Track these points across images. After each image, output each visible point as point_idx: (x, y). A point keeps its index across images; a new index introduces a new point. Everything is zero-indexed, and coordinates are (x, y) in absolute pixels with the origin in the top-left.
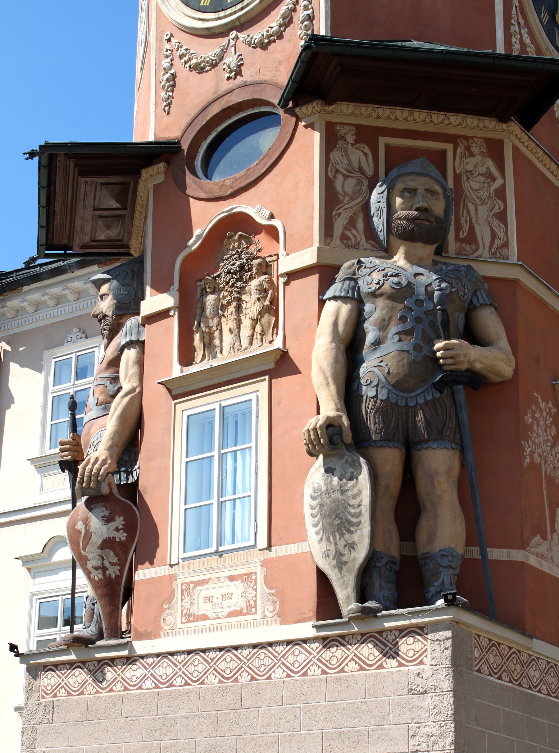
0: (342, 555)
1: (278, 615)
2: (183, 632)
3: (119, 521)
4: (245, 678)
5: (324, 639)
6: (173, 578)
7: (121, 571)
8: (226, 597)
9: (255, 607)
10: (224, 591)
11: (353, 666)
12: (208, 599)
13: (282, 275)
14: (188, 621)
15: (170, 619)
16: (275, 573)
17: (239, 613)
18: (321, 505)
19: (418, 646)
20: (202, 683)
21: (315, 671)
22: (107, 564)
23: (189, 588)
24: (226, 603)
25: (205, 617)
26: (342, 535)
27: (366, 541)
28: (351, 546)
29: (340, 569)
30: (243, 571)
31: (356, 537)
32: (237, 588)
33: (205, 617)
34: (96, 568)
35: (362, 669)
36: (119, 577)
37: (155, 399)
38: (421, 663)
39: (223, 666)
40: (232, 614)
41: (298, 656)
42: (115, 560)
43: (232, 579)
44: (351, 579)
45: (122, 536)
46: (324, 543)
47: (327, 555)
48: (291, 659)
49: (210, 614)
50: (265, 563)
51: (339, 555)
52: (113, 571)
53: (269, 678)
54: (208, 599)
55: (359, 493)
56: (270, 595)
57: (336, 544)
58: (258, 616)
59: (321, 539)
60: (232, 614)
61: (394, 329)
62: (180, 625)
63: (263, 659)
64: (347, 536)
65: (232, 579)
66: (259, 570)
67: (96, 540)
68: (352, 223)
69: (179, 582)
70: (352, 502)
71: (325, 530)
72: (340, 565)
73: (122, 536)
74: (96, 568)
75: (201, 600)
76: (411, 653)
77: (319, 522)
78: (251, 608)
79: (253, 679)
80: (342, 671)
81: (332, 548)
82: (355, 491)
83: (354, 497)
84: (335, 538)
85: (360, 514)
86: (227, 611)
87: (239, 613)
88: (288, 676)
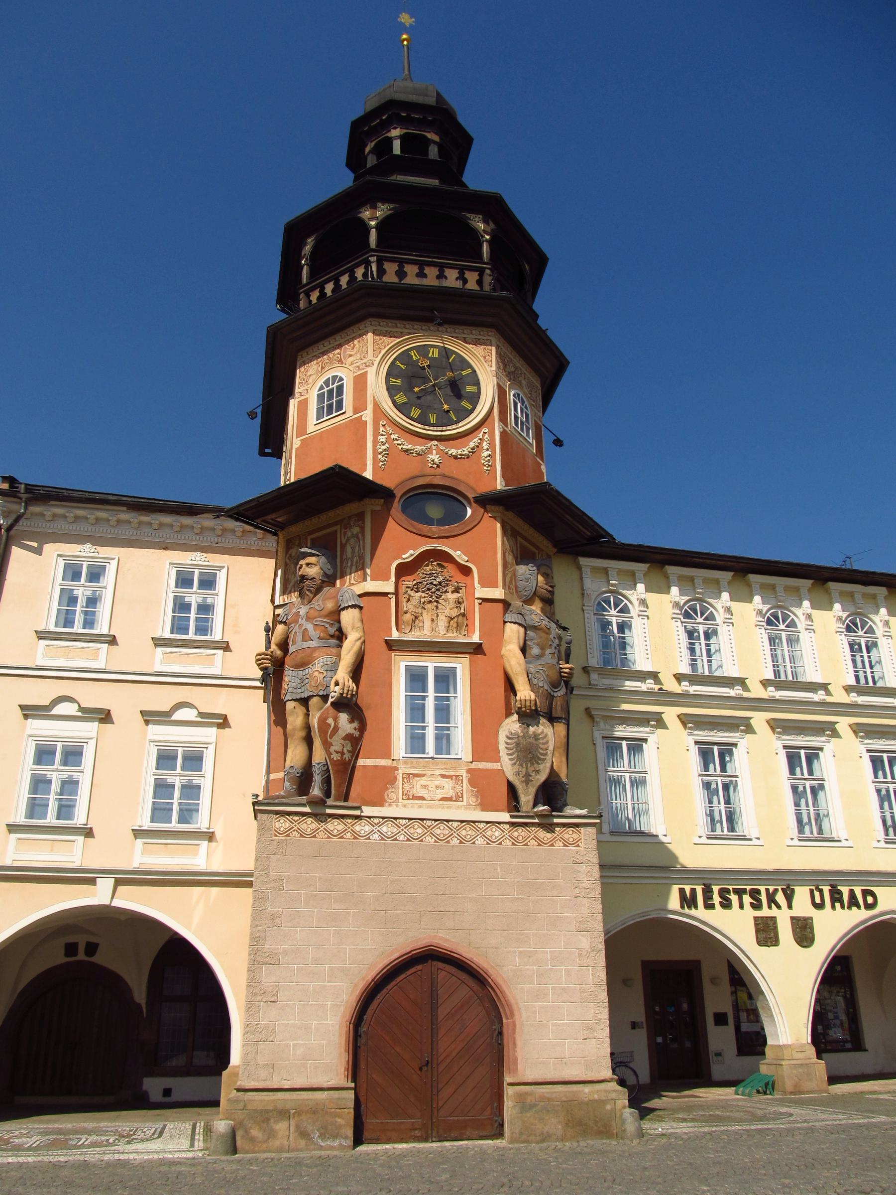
0: (530, 776)
1: (480, 804)
2: (405, 806)
3: (356, 724)
4: (455, 841)
6: (396, 768)
7: (352, 757)
9: (462, 797)
10: (437, 783)
12: (425, 787)
13: (478, 599)
14: (409, 799)
15: (393, 795)
16: (475, 777)
17: (450, 799)
18: (518, 744)
19: (575, 836)
20: (422, 841)
22: (345, 751)
23: (408, 777)
24: (439, 791)
25: (422, 798)
26: (532, 764)
27: (548, 771)
28: (538, 772)
29: (527, 784)
30: (453, 773)
31: (541, 767)
32: (448, 784)
33: (422, 798)
34: (337, 752)
35: (539, 845)
36: (350, 761)
37: (376, 650)
38: (578, 846)
39: (438, 831)
40: (443, 799)
41: (495, 833)
42: (350, 748)
43: (443, 776)
44: (532, 790)
45: (357, 734)
46: (516, 767)
47: (517, 774)
48: (489, 833)
49: (426, 796)
50: (469, 771)
51: (527, 775)
52: (347, 756)
53: (474, 843)
54: (425, 787)
55: (547, 742)
56: (473, 791)
57: (527, 768)
58: (465, 803)
59: (514, 764)
60: (443, 799)
61: (548, 651)
62: (401, 800)
63: (467, 832)
64: (536, 765)
65: (443, 776)
66: (464, 775)
67: (341, 733)
68: (511, 580)
69: (400, 772)
70: (542, 746)
71: (518, 758)
72: (527, 781)
73: (357, 734)
74: (337, 752)
75: (419, 787)
76: (571, 840)
77: (513, 753)
78: (459, 797)
79: (461, 842)
80: (526, 845)
81: (524, 770)
82: (545, 740)
83: (544, 744)
84: (527, 765)
85: (546, 754)
86: (440, 796)
87: (450, 799)
88: (488, 844)
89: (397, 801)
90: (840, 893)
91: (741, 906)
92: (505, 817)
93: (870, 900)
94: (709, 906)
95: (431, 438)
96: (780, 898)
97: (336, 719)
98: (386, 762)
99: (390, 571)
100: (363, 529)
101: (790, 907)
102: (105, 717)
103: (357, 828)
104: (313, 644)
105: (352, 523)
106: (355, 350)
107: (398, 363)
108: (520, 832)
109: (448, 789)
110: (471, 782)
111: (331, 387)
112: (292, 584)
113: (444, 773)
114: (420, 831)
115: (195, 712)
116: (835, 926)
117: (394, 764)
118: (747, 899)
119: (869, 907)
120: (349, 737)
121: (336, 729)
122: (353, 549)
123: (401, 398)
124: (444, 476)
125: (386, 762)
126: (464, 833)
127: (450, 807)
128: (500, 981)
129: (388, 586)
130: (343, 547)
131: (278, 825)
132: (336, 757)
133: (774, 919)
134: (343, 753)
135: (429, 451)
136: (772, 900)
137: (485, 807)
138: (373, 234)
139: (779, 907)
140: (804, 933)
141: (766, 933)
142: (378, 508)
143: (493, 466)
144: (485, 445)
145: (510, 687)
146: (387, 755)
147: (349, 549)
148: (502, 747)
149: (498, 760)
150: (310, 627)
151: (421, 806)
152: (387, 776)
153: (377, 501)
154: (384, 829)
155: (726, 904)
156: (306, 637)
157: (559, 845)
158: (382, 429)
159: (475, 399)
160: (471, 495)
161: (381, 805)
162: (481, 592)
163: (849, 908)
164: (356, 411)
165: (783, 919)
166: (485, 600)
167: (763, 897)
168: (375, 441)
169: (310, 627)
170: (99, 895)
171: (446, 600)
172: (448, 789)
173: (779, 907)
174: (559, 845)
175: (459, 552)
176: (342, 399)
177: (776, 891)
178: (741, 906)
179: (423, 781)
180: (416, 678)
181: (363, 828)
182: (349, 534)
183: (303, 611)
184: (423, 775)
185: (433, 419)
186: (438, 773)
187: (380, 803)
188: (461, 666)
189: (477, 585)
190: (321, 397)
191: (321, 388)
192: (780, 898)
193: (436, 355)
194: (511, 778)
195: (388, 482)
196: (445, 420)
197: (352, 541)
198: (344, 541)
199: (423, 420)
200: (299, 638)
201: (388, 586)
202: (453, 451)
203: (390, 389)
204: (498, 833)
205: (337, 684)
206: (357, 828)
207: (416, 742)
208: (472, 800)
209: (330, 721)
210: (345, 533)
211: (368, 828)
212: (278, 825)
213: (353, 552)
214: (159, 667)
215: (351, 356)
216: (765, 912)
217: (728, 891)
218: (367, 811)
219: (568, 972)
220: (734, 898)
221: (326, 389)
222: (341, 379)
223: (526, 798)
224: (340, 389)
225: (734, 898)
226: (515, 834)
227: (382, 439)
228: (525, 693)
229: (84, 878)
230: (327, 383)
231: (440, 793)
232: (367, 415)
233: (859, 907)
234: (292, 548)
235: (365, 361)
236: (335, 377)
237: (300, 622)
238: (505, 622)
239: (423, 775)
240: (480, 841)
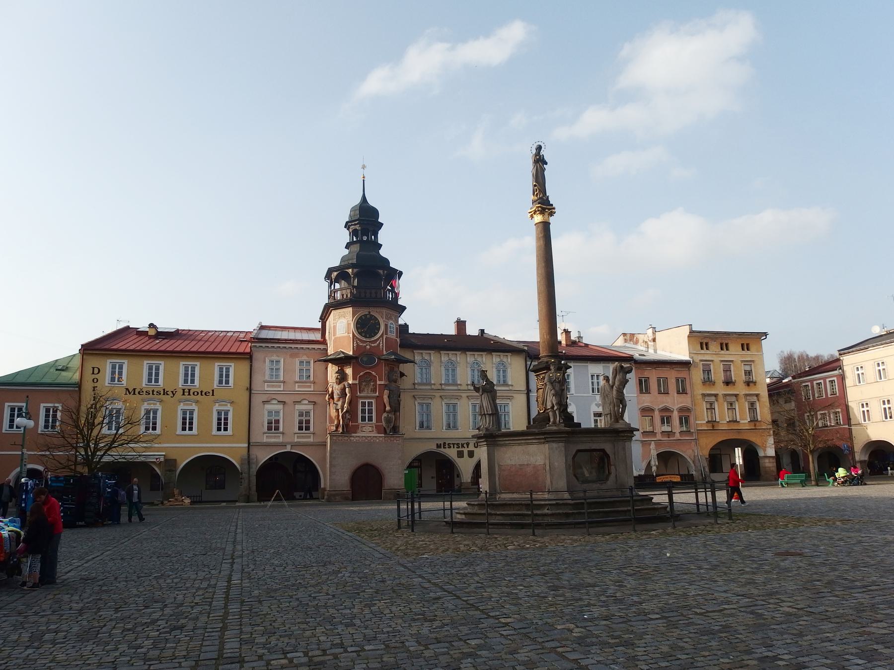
102: (284, 403)
109: (370, 429)
136: (463, 446)
141: (460, 455)
145: (385, 407)
152: (357, 427)
155: (450, 447)
159: (379, 329)
165: (466, 451)
170: (288, 449)
172: (370, 429)
180: (364, 404)
188: (373, 401)
196: (371, 337)
199: (365, 337)
207: (363, 419)
223: (388, 431)
228: (388, 408)
229: (283, 445)
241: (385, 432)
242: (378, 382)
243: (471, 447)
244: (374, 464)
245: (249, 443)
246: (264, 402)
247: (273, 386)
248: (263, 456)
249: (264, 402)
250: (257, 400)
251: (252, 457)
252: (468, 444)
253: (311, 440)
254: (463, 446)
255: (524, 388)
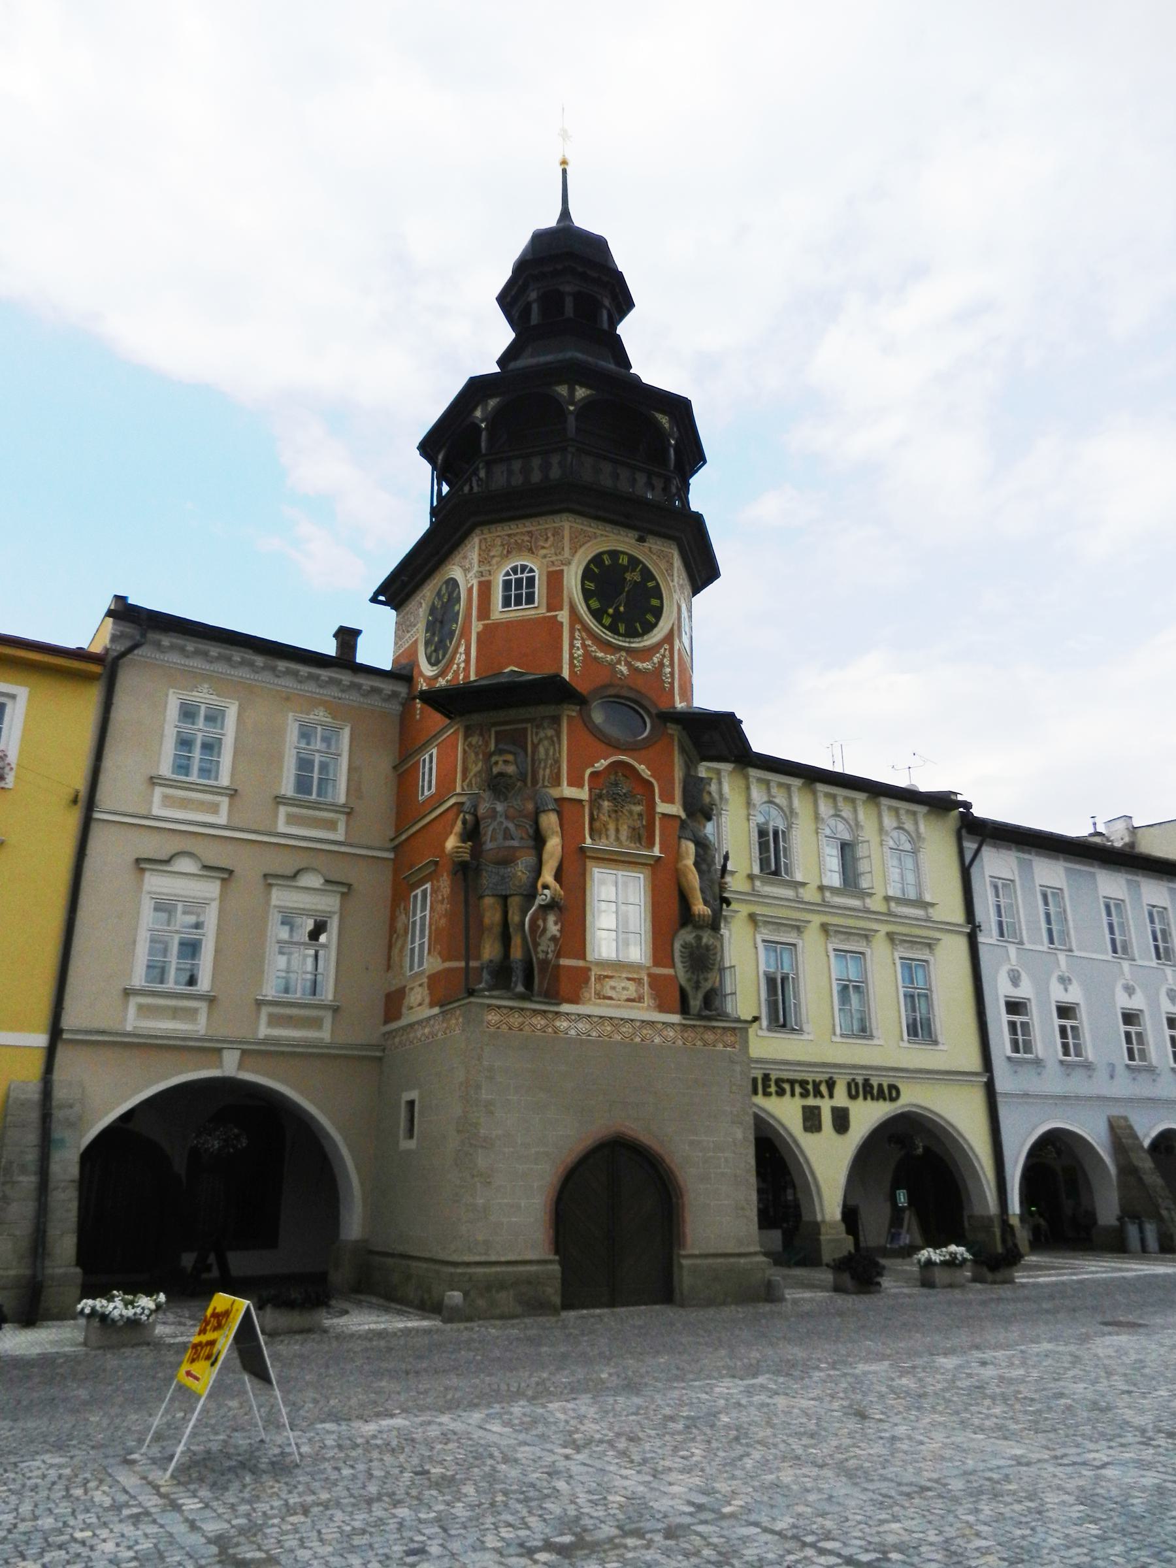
2: (595, 1004)
5: (684, 1025)
6: (589, 969)
8: (624, 988)
11: (699, 1043)
12: (613, 988)
15: (586, 995)
19: (733, 1039)
21: (680, 1042)
23: (600, 978)
25: (610, 998)
28: (706, 980)
32: (632, 986)
33: (610, 998)
40: (628, 1000)
45: (558, 934)
46: (689, 975)
47: (689, 980)
50: (649, 975)
54: (613, 988)
60: (628, 1000)
65: (629, 979)
67: (549, 935)
73: (558, 934)
78: (640, 999)
89: (590, 999)
90: (872, 1087)
91: (793, 1095)
92: (675, 1018)
93: (894, 1094)
94: (766, 1094)
95: (621, 648)
96: (824, 1089)
97: (545, 920)
98: (581, 963)
99: (583, 778)
100: (558, 734)
101: (831, 1096)
103: (558, 1024)
104: (515, 843)
105: (545, 724)
106: (549, 543)
107: (592, 566)
108: (689, 1034)
110: (651, 986)
111: (519, 576)
112: (472, 774)
113: (630, 976)
114: (609, 1028)
115: (322, 881)
116: (867, 1116)
117: (588, 965)
118: (798, 1090)
119: (892, 1099)
120: (554, 939)
121: (545, 930)
122: (547, 751)
123: (595, 604)
124: (631, 689)
125: (581, 963)
126: (645, 1032)
127: (632, 1008)
128: (673, 1166)
129: (583, 794)
130: (535, 747)
131: (490, 1017)
132: (541, 956)
133: (818, 1108)
134: (547, 953)
135: (619, 662)
137: (662, 1008)
138: (572, 422)
139: (822, 1096)
140: (841, 1121)
141: (812, 1121)
142: (574, 714)
143: (672, 684)
144: (666, 662)
146: (583, 956)
147: (541, 750)
148: (677, 954)
149: (673, 966)
150: (511, 826)
151: (609, 1006)
152: (582, 976)
153: (573, 707)
154: (580, 1025)
155: (781, 1093)
156: (507, 835)
157: (720, 1047)
158: (577, 633)
160: (654, 711)
161: (577, 1003)
162: (662, 808)
163: (878, 1099)
164: (549, 609)
165: (825, 1106)
166: (664, 815)
167: (810, 1087)
168: (572, 646)
169: (511, 826)
170: (229, 1066)
171: (631, 812)
173: (822, 1096)
174: (720, 1047)
175: (643, 767)
176: (534, 593)
177: (821, 1082)
178: (793, 1095)
179: (612, 983)
181: (563, 1024)
182: (542, 735)
183: (500, 807)
184: (611, 977)
185: (622, 629)
186: (624, 975)
187: (575, 1001)
189: (657, 800)
190: (507, 585)
191: (508, 574)
192: (824, 1089)
193: (625, 562)
194: (683, 982)
195: (583, 687)
196: (632, 634)
197: (546, 743)
198: (536, 741)
199: (613, 629)
200: (500, 836)
201: (583, 794)
202: (639, 665)
203: (587, 595)
204: (671, 1034)
205: (546, 887)
206: (558, 1024)
208: (652, 1002)
209: (540, 922)
210: (537, 734)
211: (565, 1024)
212: (490, 1017)
213: (547, 753)
214: (282, 827)
215: (543, 548)
216: (811, 1101)
217: (783, 1081)
218: (566, 1008)
219: (726, 1160)
220: (787, 1087)
221: (513, 577)
222: (532, 570)
224: (531, 581)
225: (787, 1087)
226: (686, 1035)
227: (578, 644)
229: (210, 1050)
230: (515, 570)
231: (625, 995)
232: (563, 616)
233: (885, 1099)
234: (471, 735)
235: (560, 557)
236: (524, 568)
237: (499, 819)
238: (680, 838)
239: (611, 977)
240: (657, 1040)
241: (684, 1010)
242: (662, 808)
243: (841, 1098)
244: (645, 1138)
245: (56, 1032)
246: (142, 864)
247: (184, 804)
248: (106, 1096)
249: (142, 864)
250: (110, 852)
251: (60, 1093)
252: (831, 1085)
253: (324, 1034)
254: (818, 1094)
255: (959, 917)
